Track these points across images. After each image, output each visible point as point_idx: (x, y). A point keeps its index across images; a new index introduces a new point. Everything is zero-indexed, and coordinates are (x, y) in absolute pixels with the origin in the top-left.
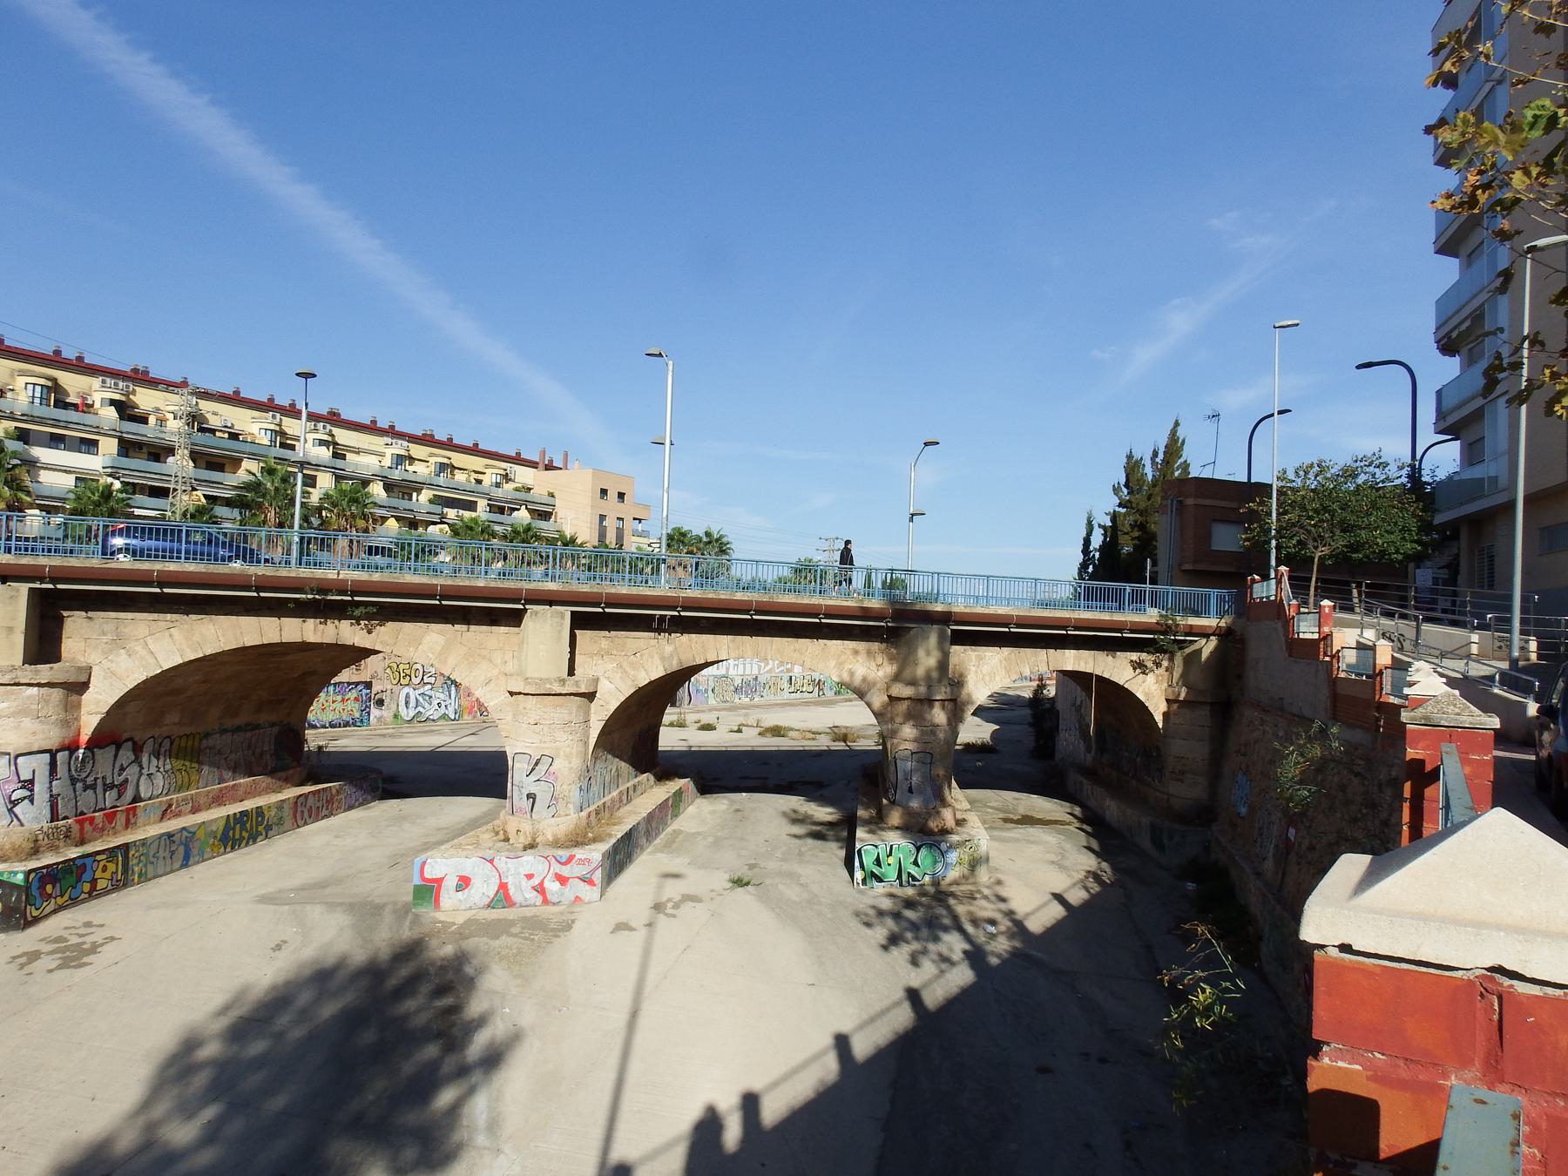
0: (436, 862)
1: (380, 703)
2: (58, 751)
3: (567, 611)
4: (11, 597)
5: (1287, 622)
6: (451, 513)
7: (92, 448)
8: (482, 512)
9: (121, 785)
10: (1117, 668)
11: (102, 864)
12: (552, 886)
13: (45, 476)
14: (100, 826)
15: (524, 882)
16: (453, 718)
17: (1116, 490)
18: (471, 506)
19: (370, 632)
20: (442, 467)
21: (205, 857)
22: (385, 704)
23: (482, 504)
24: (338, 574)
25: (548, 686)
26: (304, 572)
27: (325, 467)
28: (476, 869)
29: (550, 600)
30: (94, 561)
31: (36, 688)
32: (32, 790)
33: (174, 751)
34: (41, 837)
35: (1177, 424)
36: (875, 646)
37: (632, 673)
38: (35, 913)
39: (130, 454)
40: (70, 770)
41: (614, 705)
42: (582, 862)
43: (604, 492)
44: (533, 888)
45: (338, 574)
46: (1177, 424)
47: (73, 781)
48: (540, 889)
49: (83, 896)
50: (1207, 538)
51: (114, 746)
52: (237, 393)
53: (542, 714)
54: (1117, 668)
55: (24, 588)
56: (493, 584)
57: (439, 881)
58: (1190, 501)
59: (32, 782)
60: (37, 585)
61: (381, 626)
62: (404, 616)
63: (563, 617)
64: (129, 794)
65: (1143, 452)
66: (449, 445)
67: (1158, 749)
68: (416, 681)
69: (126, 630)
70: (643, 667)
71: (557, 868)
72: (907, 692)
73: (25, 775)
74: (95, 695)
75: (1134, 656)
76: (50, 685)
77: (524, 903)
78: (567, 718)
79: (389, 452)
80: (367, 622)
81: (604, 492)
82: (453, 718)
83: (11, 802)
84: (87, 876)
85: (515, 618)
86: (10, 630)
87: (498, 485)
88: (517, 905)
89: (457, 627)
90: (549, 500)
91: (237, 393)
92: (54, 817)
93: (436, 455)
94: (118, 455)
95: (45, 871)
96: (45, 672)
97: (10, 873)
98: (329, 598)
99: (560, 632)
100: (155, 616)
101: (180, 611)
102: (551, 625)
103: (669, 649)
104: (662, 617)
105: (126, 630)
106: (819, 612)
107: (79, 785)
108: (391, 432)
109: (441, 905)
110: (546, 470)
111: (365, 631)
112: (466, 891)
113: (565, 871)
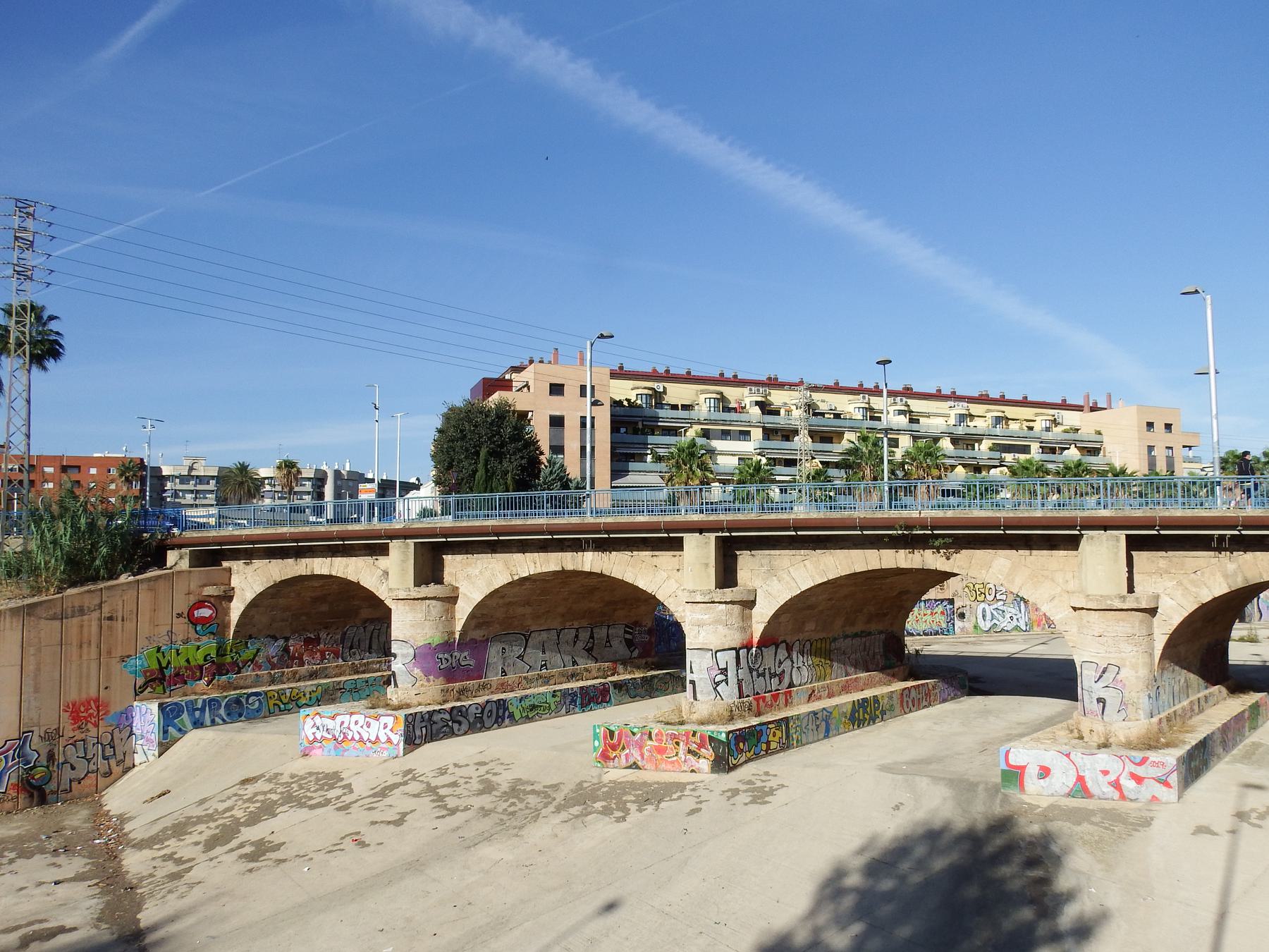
0: (1019, 752)
1: (962, 616)
2: (740, 649)
3: (1122, 535)
4: (706, 543)
6: (1009, 457)
7: (747, 437)
8: (1035, 453)
9: (780, 674)
11: (772, 730)
12: (1128, 784)
13: (721, 460)
14: (769, 703)
15: (1100, 776)
16: (1024, 629)
18: (1025, 449)
19: (948, 559)
20: (998, 420)
21: (840, 731)
22: (966, 617)
23: (1035, 447)
24: (920, 513)
25: (1109, 602)
26: (893, 513)
27: (904, 431)
28: (1055, 762)
30: (753, 515)
31: (724, 605)
32: (726, 676)
33: (813, 651)
34: (734, 709)
37: (1194, 590)
38: (734, 762)
39: (770, 438)
40: (748, 662)
41: (1177, 620)
42: (1155, 764)
43: (1150, 425)
44: (1109, 783)
45: (920, 513)
47: (751, 670)
48: (1117, 785)
49: (763, 753)
51: (774, 646)
53: (1105, 627)
55: (712, 536)
56: (1049, 514)
57: (1023, 768)
59: (726, 669)
60: (720, 534)
61: (957, 553)
62: (975, 545)
63: (1118, 539)
64: (786, 681)
66: (1003, 401)
68: (990, 598)
69: (776, 563)
70: (1205, 584)
71: (1131, 768)
73: (722, 666)
74: (760, 610)
76: (732, 603)
77: (1102, 796)
78: (1130, 631)
79: (953, 413)
80: (945, 551)
82: (1024, 629)
83: (715, 683)
84: (764, 739)
85: (1072, 543)
86: (707, 565)
87: (1048, 429)
88: (1096, 797)
89: (1021, 552)
90: (1098, 438)
92: (741, 696)
94: (763, 440)
95: (738, 732)
96: (729, 594)
97: (718, 732)
98: (915, 532)
99: (1116, 554)
100: (793, 552)
101: (810, 547)
102: (1107, 548)
103: (1231, 567)
104: (1222, 537)
105: (776, 563)
106: (1237, 524)
107: (755, 673)
108: (954, 397)
109: (1026, 788)
110: (1091, 411)
111: (944, 558)
112: (1047, 779)
113: (1140, 771)
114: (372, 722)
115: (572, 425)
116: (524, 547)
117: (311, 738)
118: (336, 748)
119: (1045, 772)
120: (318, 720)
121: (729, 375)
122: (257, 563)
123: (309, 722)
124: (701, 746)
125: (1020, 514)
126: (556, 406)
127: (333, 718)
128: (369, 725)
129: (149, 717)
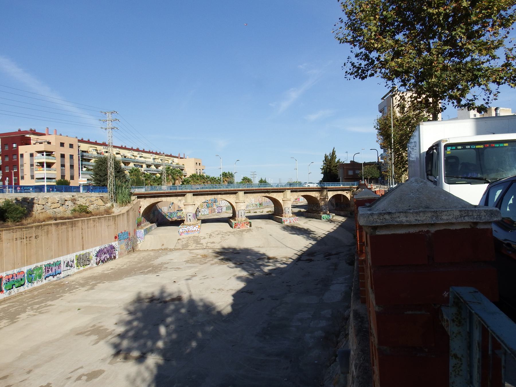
1: (200, 212)
5: (367, 187)
10: (344, 193)
12: (294, 221)
20: (154, 159)
29: (288, 189)
35: (334, 148)
36: (318, 192)
43: (196, 163)
46: (334, 148)
48: (293, 221)
50: (347, 173)
52: (89, 140)
54: (344, 193)
55: (243, 192)
58: (345, 167)
65: (328, 154)
67: (349, 204)
68: (203, 207)
72: (323, 197)
75: (346, 191)
79: (152, 158)
81: (196, 163)
85: (184, 195)
87: (172, 163)
90: (183, 166)
91: (89, 140)
93: (161, 157)
108: (153, 153)
110: (181, 158)
114: (194, 227)
115: (67, 157)
116: (208, 194)
117: (181, 232)
118: (187, 233)
120: (183, 228)
121: (124, 147)
122: (147, 199)
124: (248, 223)
125: (248, 189)
126: (63, 151)
127: (186, 227)
128: (193, 228)
129: (141, 233)
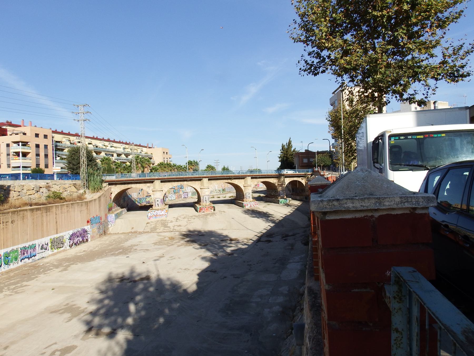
1: (167, 197)
5: (320, 173)
12: (255, 205)
17: (281, 150)
20: (124, 148)
35: (290, 138)
43: (164, 152)
46: (290, 138)
48: (254, 205)
52: (62, 131)
58: (300, 156)
65: (285, 144)
66: (114, 141)
67: (304, 189)
72: (280, 183)
75: (301, 178)
79: (122, 147)
81: (164, 152)
85: (152, 182)
87: (141, 152)
91: (62, 131)
93: (130, 147)
108: (123, 143)
115: (42, 147)
116: (174, 181)
117: (150, 216)
119: (248, 205)
120: (151, 213)
121: (95, 137)
122: (118, 186)
123: (150, 213)
125: (212, 176)
126: (37, 141)
127: (154, 212)
129: (112, 217)
